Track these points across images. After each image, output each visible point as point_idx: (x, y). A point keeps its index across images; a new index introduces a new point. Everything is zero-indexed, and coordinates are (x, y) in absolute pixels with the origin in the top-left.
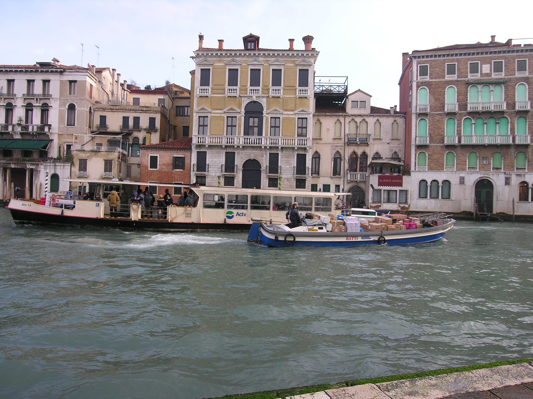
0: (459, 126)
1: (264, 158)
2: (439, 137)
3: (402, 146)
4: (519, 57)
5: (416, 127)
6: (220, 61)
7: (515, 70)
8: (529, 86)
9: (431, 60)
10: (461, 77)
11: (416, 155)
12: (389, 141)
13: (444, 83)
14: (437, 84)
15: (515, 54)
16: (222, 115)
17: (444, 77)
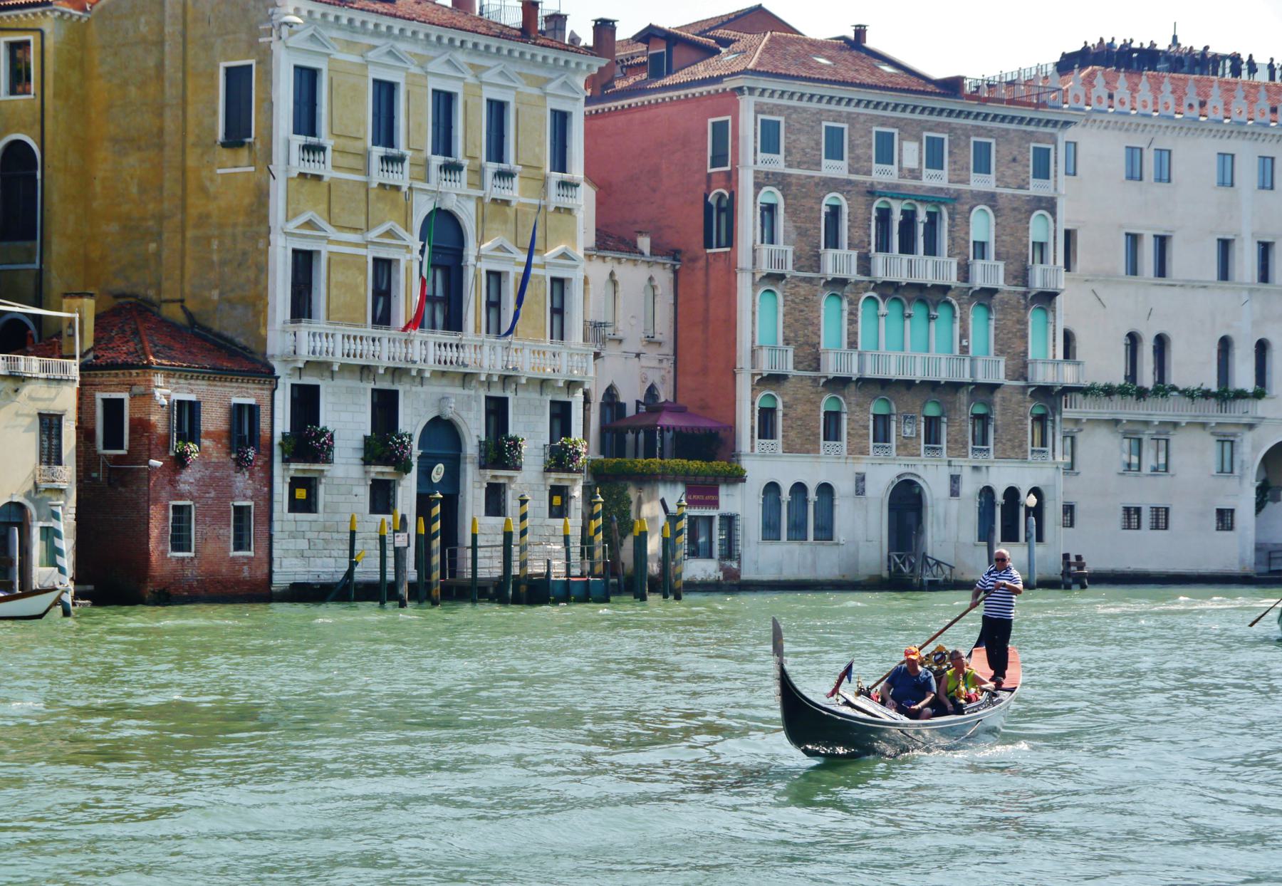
0: (853, 321)
1: (472, 415)
2: (809, 350)
3: (668, 365)
4: (978, 131)
5: (754, 313)
6: (350, 45)
7: (968, 169)
8: (996, 217)
9: (789, 107)
10: (857, 172)
11: (753, 403)
12: (639, 348)
13: (817, 184)
14: (803, 186)
15: (970, 122)
16: (362, 251)
17: (818, 164)
